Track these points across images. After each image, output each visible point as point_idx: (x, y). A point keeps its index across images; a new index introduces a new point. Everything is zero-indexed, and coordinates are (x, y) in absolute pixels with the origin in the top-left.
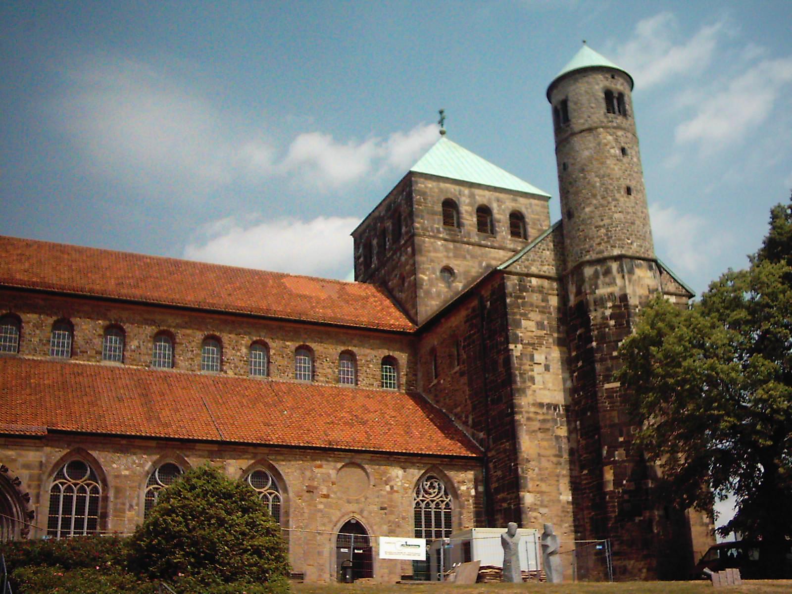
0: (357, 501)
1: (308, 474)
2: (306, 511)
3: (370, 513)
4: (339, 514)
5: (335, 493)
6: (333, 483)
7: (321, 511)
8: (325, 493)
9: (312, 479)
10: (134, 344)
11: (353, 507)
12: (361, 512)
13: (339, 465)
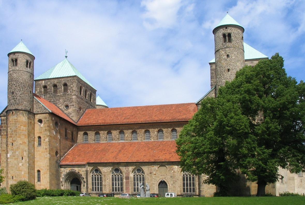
0: (164, 175)
1: (150, 169)
2: (150, 178)
3: (168, 178)
4: (159, 179)
5: (158, 173)
6: (157, 171)
7: (154, 178)
8: (155, 173)
9: (151, 170)
10: (126, 135)
11: (163, 177)
12: (165, 178)
13: (158, 166)
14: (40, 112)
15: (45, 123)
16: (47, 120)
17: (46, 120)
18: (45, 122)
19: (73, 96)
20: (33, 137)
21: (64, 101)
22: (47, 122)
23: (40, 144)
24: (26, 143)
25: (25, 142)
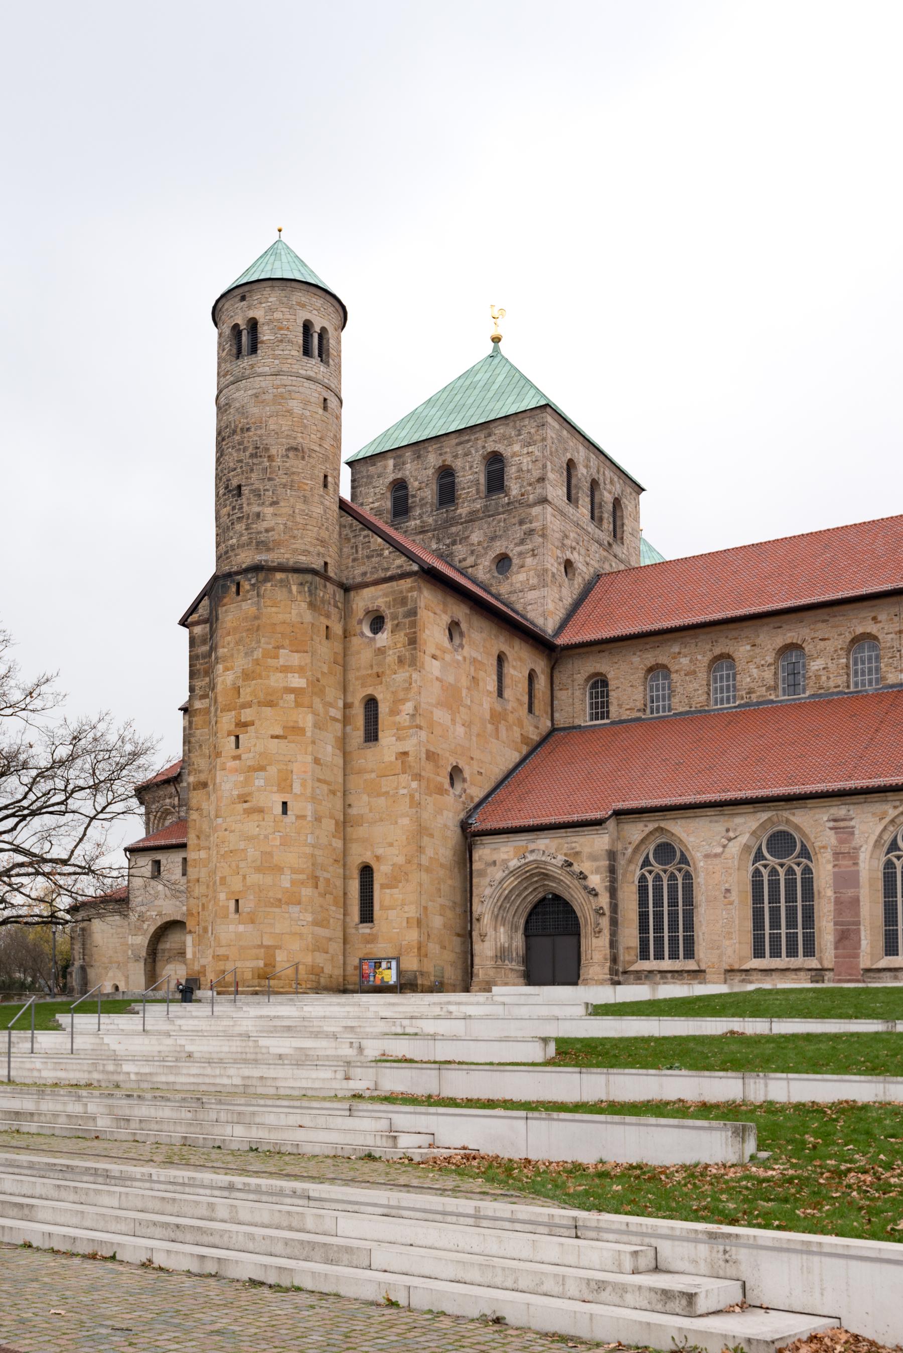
14: (369, 578)
15: (397, 625)
16: (406, 609)
17: (401, 610)
18: (396, 622)
19: (530, 506)
20: (340, 704)
21: (493, 539)
22: (407, 620)
23: (372, 735)
24: (301, 731)
25: (301, 725)
